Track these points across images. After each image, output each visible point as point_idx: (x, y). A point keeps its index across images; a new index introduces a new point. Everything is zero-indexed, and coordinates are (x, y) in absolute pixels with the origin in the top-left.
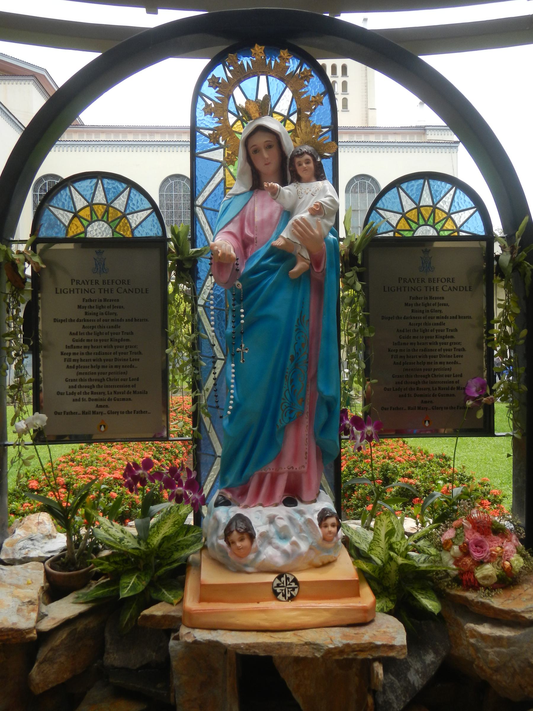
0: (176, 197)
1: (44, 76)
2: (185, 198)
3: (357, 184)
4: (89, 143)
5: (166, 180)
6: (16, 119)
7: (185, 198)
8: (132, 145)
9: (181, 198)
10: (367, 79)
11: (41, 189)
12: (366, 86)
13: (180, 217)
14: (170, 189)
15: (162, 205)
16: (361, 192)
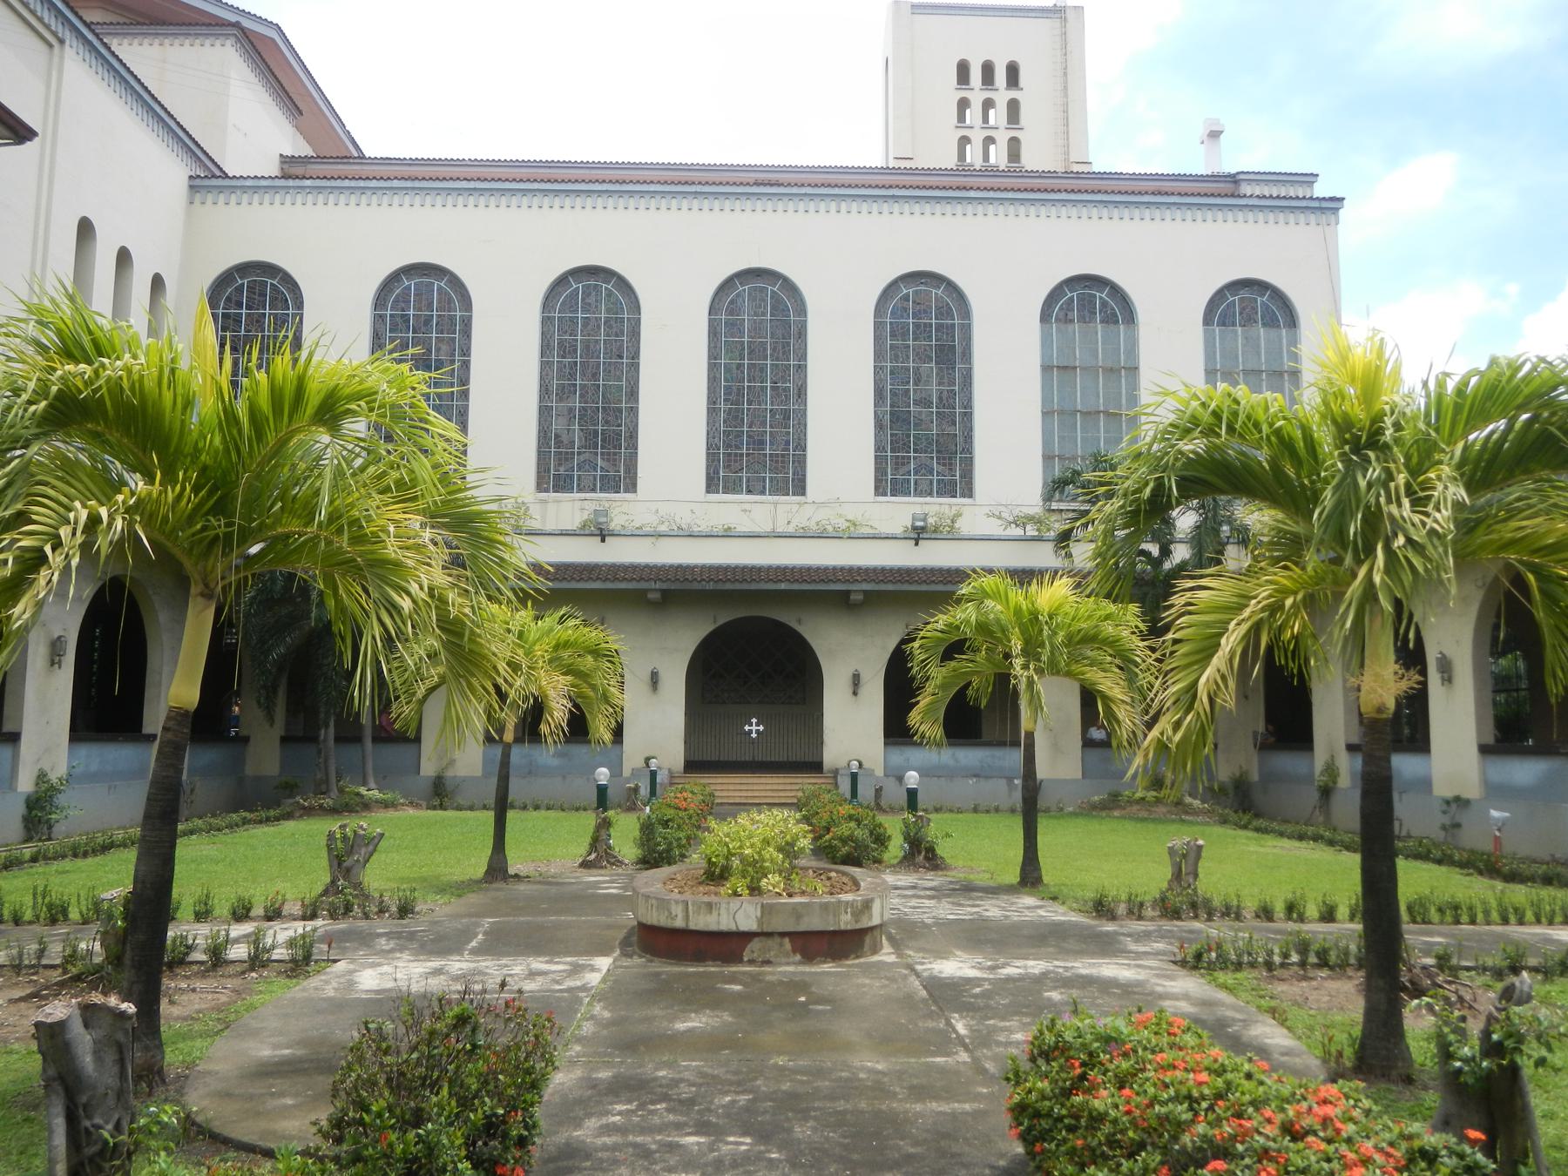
0: (585, 325)
1: (273, 40)
2: (610, 327)
3: (1072, 299)
4: (362, 184)
5: (562, 281)
6: (171, 116)
7: (610, 327)
8: (475, 189)
9: (599, 327)
10: (1066, 96)
11: (229, 299)
12: (1066, 111)
13: (595, 376)
14: (571, 303)
15: (548, 345)
16: (1082, 319)
